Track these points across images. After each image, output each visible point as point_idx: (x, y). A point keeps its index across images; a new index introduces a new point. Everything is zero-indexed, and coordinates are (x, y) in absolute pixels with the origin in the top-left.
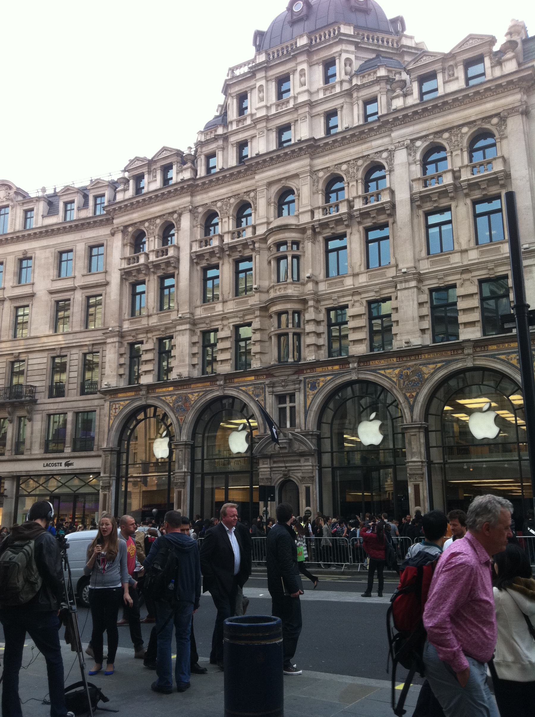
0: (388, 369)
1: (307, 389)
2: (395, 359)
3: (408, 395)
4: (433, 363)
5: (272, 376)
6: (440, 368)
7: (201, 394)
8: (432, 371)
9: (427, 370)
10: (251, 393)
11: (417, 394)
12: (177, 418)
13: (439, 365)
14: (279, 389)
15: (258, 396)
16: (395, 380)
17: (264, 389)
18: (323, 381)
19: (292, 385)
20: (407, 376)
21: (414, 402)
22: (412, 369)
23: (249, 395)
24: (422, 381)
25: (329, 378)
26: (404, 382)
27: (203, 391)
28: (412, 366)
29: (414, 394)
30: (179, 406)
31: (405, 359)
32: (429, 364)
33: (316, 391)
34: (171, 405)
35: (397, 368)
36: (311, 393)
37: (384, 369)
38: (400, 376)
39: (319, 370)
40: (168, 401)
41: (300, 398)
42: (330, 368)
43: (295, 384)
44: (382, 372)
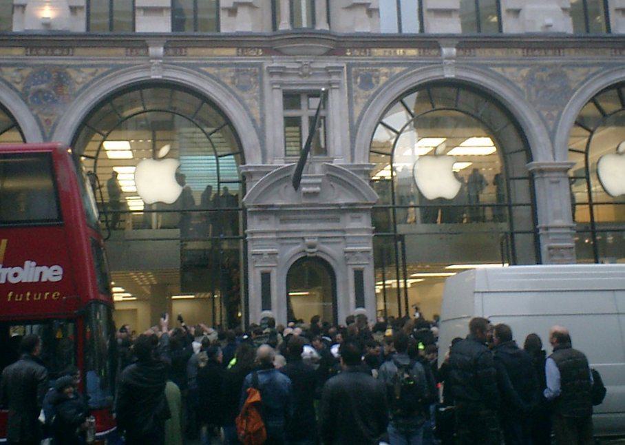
0: (509, 65)
1: (354, 86)
2: (520, 51)
3: (545, 114)
4: (584, 66)
5: (278, 52)
6: (594, 74)
7: (100, 71)
8: (583, 78)
9: (575, 75)
10: (228, 81)
11: (560, 113)
12: (36, 117)
13: (594, 70)
14: (295, 82)
15: (244, 89)
16: (521, 85)
17: (259, 77)
18: (386, 74)
19: (322, 75)
20: (542, 81)
21: (556, 126)
22: (550, 71)
23: (224, 85)
24: (567, 92)
25: (398, 70)
26: (537, 92)
27: (106, 65)
28: (551, 66)
29: (555, 113)
30: (40, 91)
31: (536, 52)
32: (578, 66)
33: (372, 92)
34: (19, 87)
35: (524, 66)
36: (362, 95)
37: (502, 65)
38: (530, 80)
39: (379, 52)
40: (9, 80)
41: (337, 101)
42: (400, 52)
43: (330, 74)
44: (499, 70)
